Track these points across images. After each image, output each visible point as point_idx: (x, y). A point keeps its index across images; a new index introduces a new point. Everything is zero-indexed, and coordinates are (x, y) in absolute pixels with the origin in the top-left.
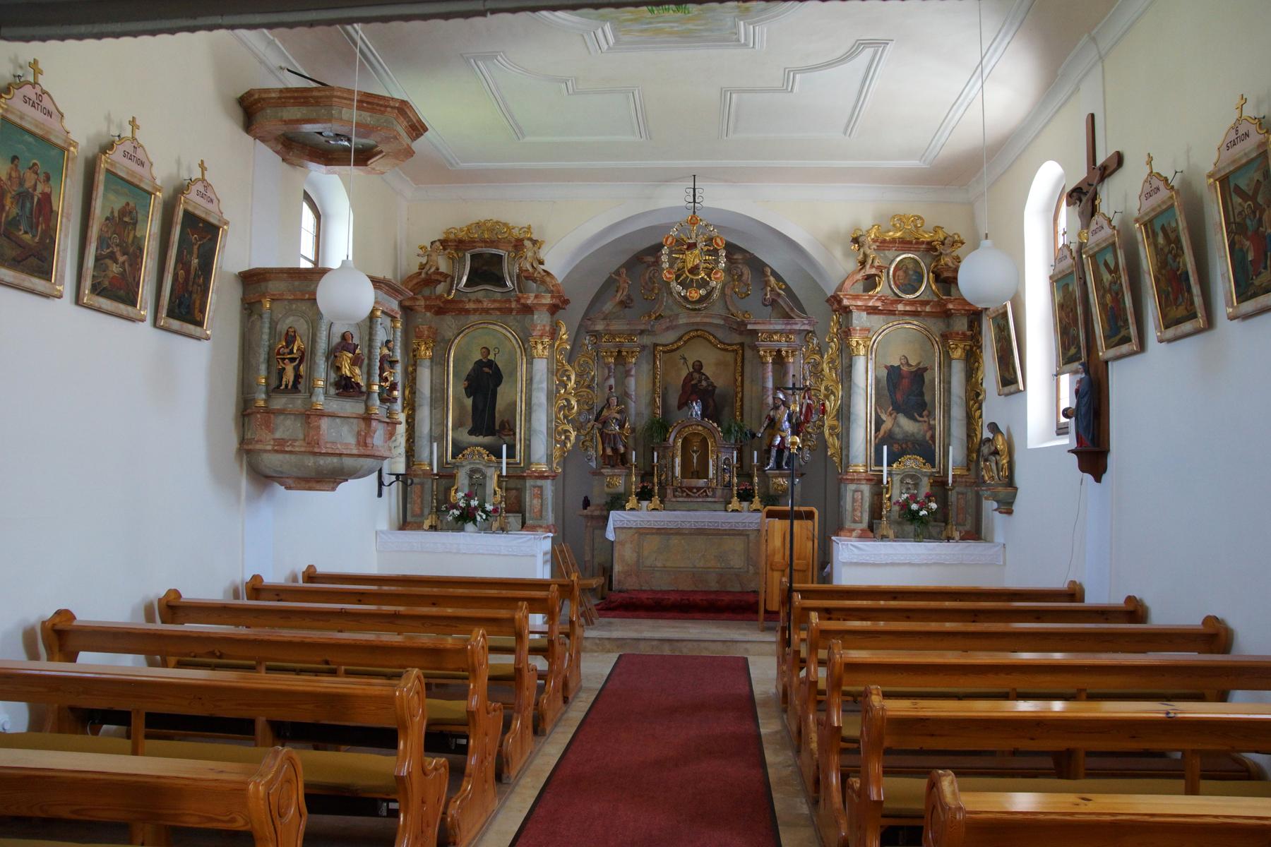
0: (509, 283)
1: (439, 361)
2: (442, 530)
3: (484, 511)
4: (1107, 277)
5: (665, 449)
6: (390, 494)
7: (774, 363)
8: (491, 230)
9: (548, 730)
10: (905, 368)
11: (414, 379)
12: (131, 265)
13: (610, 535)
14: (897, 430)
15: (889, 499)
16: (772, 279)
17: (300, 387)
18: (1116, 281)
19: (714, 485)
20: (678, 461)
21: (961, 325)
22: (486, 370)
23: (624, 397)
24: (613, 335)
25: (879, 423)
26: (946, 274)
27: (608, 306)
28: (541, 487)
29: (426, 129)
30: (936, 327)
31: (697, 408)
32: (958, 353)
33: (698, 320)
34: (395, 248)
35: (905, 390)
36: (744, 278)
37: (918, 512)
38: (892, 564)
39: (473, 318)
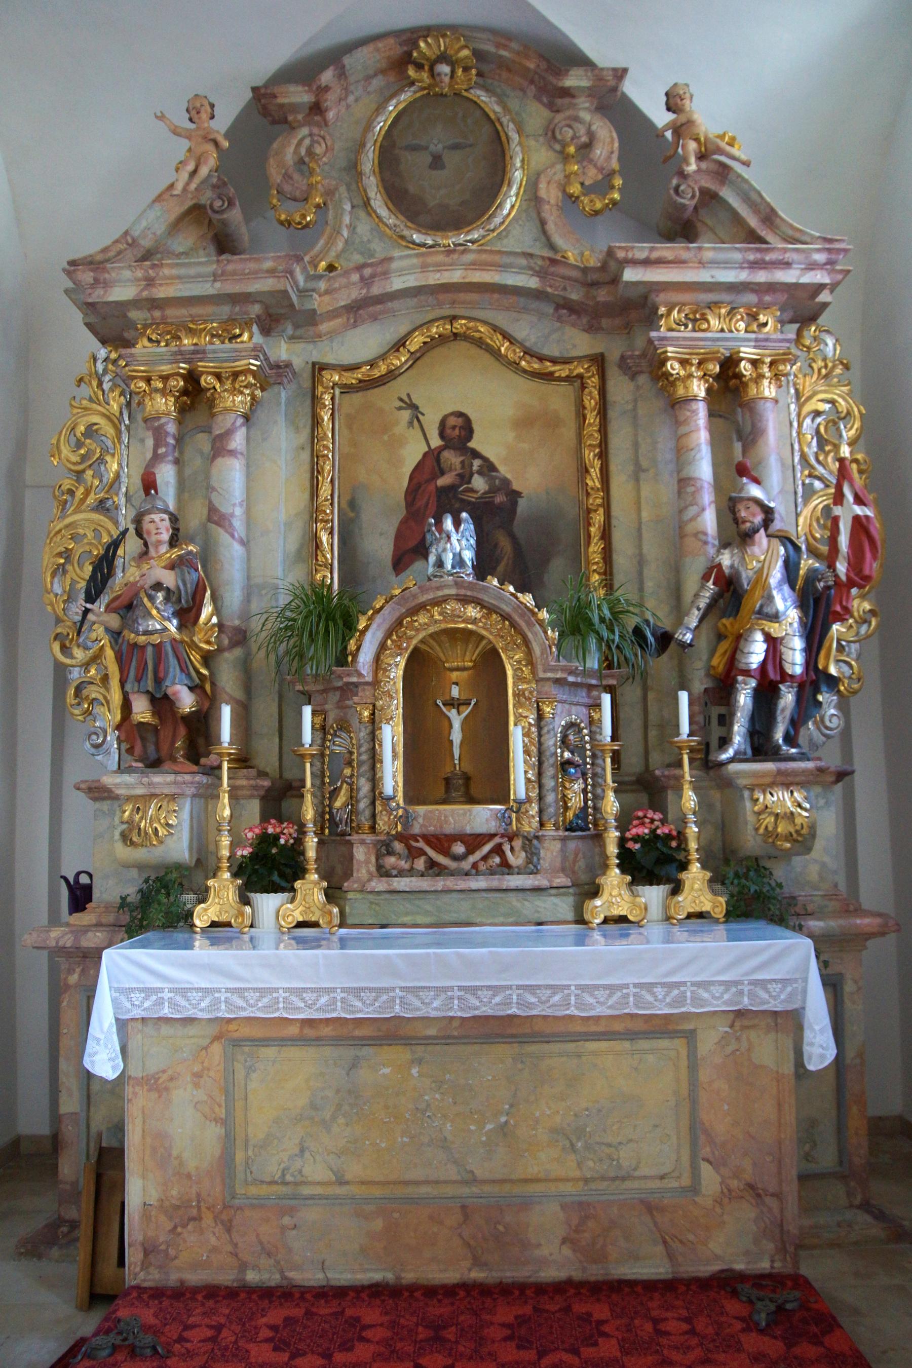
5: (338, 693)
13: (103, 1059)
19: (530, 825)
20: (391, 735)
31: (458, 543)
36: (599, 152)
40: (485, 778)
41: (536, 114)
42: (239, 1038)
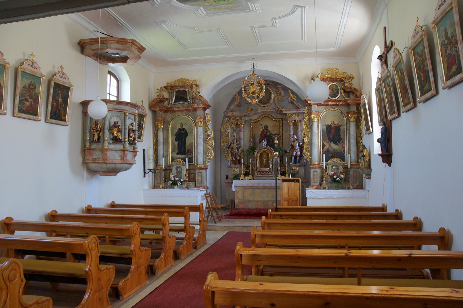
0: (189, 101)
1: (166, 129)
2: (167, 188)
3: (181, 182)
4: (388, 89)
6: (149, 176)
7: (293, 125)
8: (182, 82)
9: (183, 258)
10: (333, 126)
11: (157, 136)
12: (34, 102)
13: (233, 189)
14: (330, 148)
15: (327, 174)
16: (291, 94)
17: (100, 140)
18: (390, 90)
20: (258, 162)
21: (353, 109)
22: (182, 131)
23: (239, 140)
24: (235, 117)
25: (324, 146)
26: (347, 90)
27: (232, 107)
28: (201, 173)
29: (145, 49)
30: (345, 110)
31: (265, 142)
32: (352, 119)
33: (265, 110)
34: (149, 89)
35: (333, 134)
36: (282, 94)
37: (336, 178)
38: (326, 198)
39: (177, 113)
40: (267, 166)
41: (275, 89)
42: (245, 188)
